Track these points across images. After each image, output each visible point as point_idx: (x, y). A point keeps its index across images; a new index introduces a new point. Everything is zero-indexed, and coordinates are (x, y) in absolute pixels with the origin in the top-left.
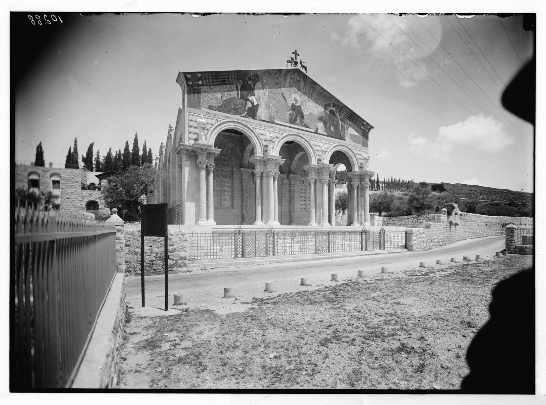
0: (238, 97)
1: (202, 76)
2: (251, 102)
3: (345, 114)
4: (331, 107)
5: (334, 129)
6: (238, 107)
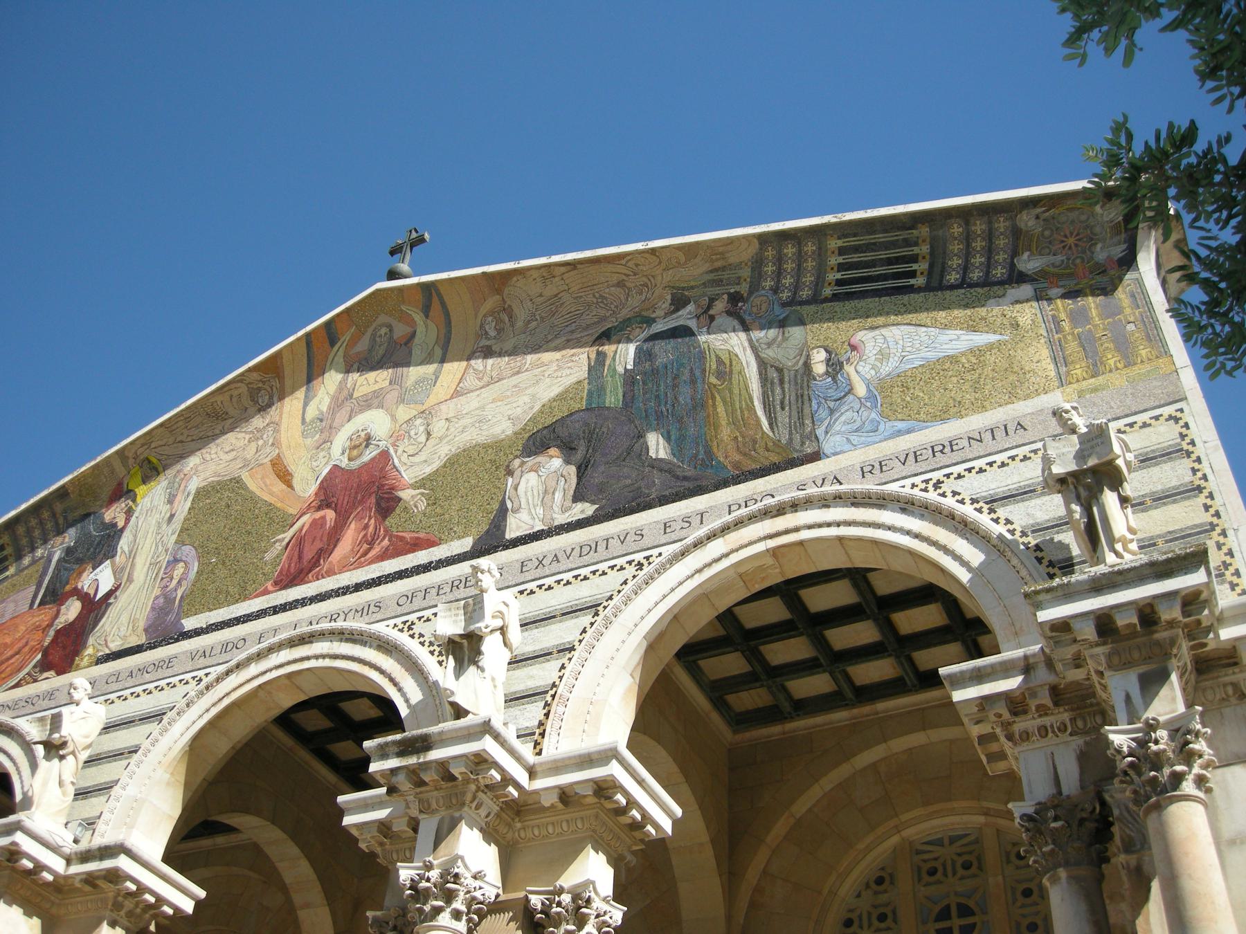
3: (797, 287)
4: (654, 320)
5: (677, 443)
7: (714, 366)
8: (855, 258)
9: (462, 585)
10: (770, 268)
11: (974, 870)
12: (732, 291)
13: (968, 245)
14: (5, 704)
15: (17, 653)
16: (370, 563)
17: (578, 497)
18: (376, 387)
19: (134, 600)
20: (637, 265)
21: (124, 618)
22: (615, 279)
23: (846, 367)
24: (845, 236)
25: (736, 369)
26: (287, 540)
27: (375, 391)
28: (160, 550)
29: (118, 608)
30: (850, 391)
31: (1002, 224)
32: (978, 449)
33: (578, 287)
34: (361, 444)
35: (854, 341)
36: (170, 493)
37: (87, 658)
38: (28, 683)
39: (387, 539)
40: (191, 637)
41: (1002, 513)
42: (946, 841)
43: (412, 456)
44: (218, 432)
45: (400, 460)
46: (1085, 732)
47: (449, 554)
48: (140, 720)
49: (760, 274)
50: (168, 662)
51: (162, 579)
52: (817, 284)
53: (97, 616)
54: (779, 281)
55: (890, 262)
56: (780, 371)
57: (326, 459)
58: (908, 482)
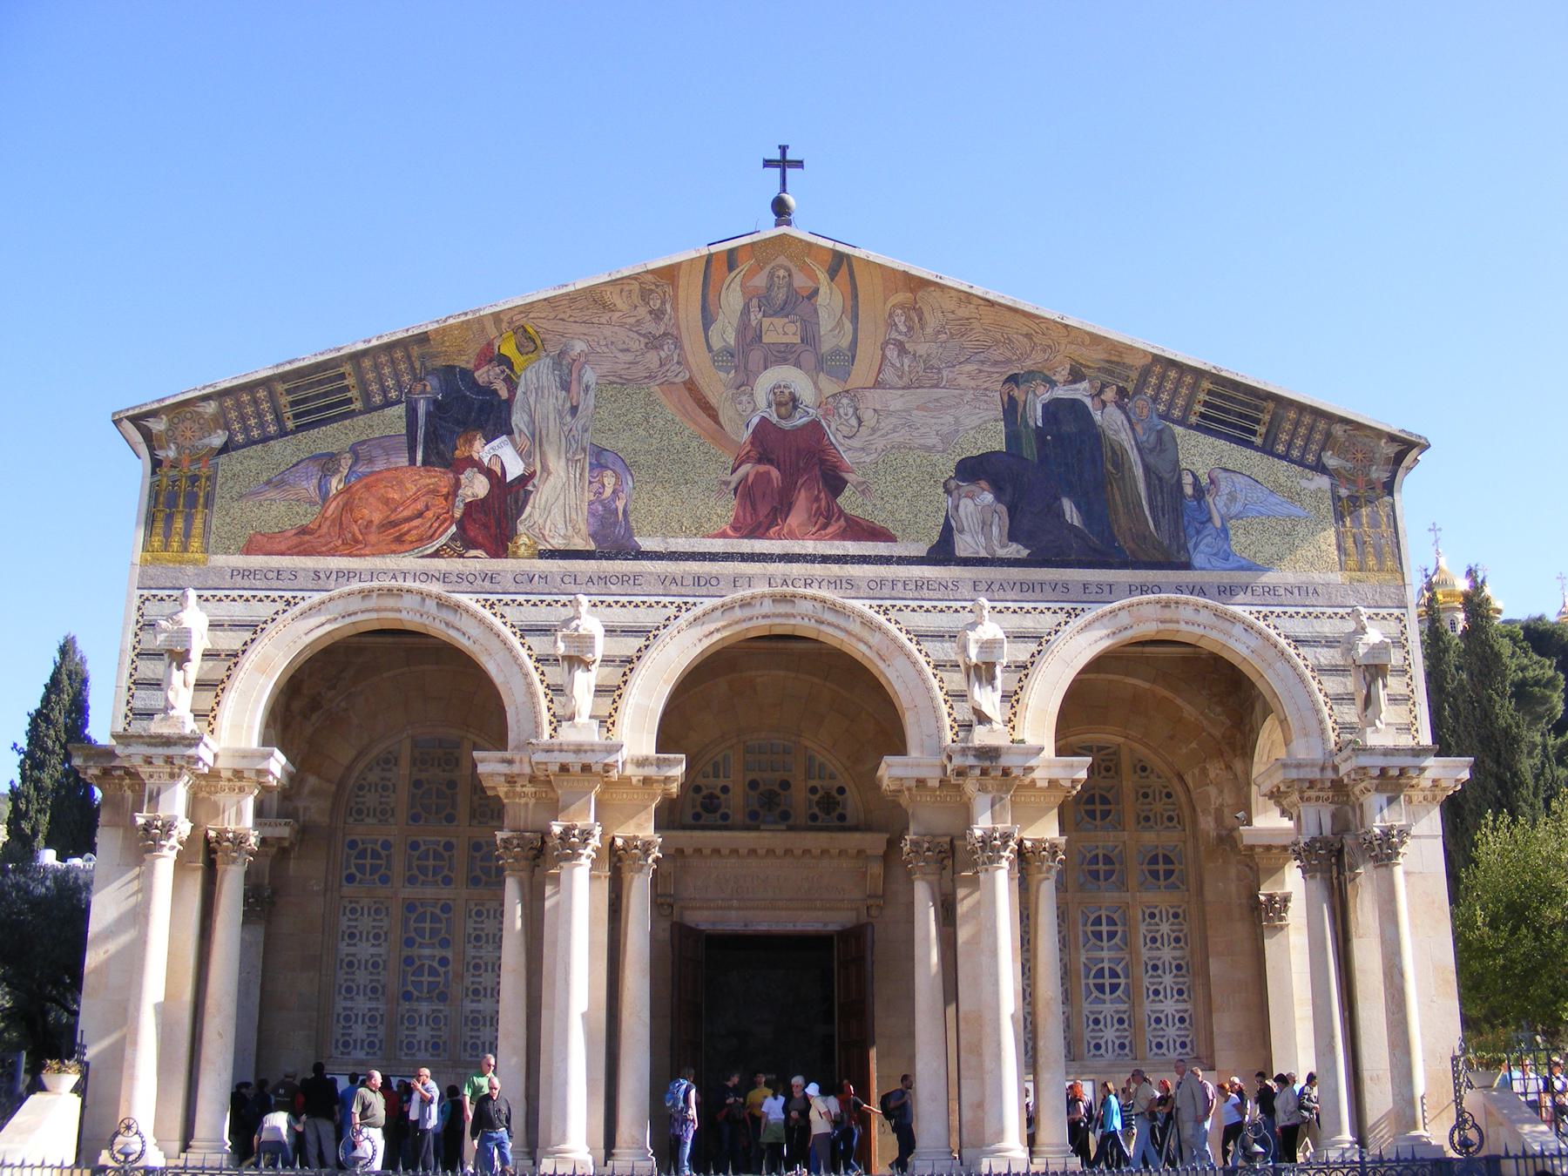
0: (412, 461)
1: (223, 412)
2: (488, 473)
3: (1171, 405)
4: (1053, 384)
6: (406, 513)
7: (1110, 454)
8: (1218, 402)
9: (925, 587)
10: (1153, 380)
11: (1112, 773)
12: (1121, 385)
13: (1296, 429)
14: (430, 574)
15: (420, 515)
16: (829, 539)
17: (1013, 536)
18: (786, 339)
19: (562, 497)
20: (1047, 329)
21: (556, 512)
22: (1025, 330)
23: (1207, 497)
24: (1216, 383)
25: (1126, 466)
26: (733, 485)
27: (787, 344)
28: (575, 446)
29: (543, 502)
30: (1210, 519)
31: (1322, 425)
32: (1287, 599)
33: (988, 321)
34: (786, 404)
35: (1214, 475)
36: (561, 378)
37: (523, 547)
38: (451, 556)
39: (842, 519)
40: (651, 559)
41: (1302, 650)
42: (1095, 749)
43: (849, 438)
44: (603, 320)
45: (835, 437)
46: (1337, 803)
47: (907, 554)
48: (622, 631)
49: (1145, 381)
50: (635, 578)
51: (590, 483)
52: (1186, 410)
53: (516, 502)
54: (1157, 394)
55: (1241, 416)
56: (1160, 479)
57: (752, 405)
58: (1248, 608)
